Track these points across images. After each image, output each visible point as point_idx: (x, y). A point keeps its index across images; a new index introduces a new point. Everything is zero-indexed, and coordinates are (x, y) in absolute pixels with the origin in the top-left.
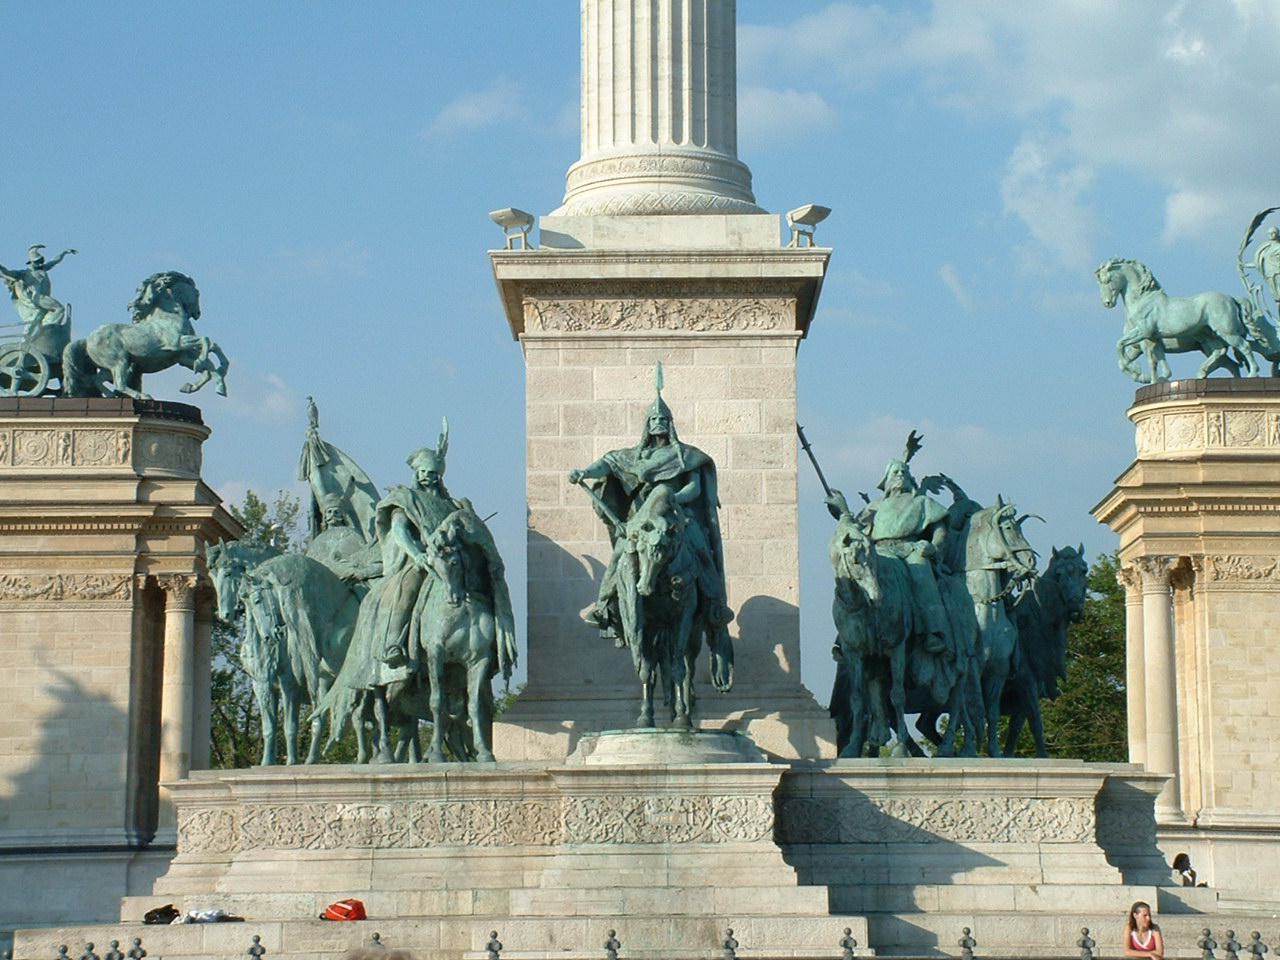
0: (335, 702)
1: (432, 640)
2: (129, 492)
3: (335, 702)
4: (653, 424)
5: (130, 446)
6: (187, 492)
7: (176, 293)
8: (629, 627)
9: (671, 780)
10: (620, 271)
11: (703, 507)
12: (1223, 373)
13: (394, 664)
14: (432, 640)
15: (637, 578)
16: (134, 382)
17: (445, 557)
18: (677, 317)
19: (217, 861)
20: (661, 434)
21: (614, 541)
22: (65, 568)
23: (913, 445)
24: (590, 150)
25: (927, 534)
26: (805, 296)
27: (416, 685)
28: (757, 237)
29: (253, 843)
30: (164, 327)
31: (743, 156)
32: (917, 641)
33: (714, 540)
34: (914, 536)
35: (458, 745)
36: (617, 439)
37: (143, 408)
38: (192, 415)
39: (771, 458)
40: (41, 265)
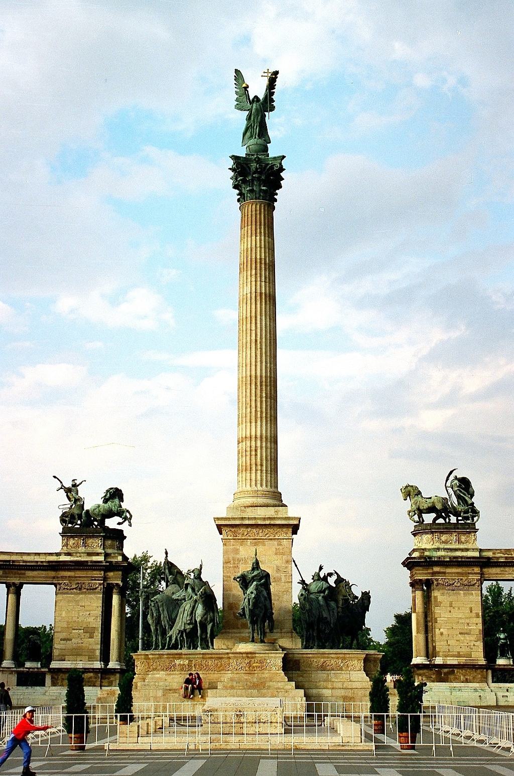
0: (173, 633)
1: (198, 620)
3: (173, 633)
4: (254, 564)
5: (102, 542)
6: (120, 558)
7: (116, 494)
8: (247, 617)
9: (257, 655)
10: (247, 522)
13: (189, 624)
14: (198, 620)
15: (249, 605)
16: (104, 522)
17: (202, 598)
18: (261, 534)
21: (244, 594)
23: (321, 568)
25: (324, 592)
27: (194, 629)
29: (154, 669)
30: (112, 505)
31: (279, 490)
33: (269, 593)
34: (320, 592)
36: (245, 568)
38: (121, 532)
39: (285, 570)
40: (75, 486)
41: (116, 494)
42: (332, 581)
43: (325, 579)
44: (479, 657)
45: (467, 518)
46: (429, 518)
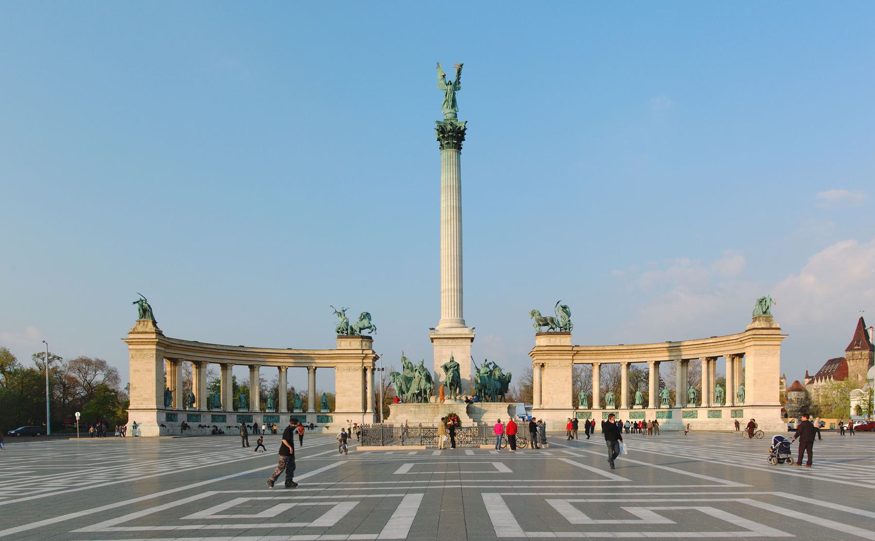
0: (409, 395)
2: (360, 352)
6: (371, 352)
11: (458, 370)
12: (551, 330)
19: (396, 415)
20: (452, 361)
22: (350, 365)
24: (443, 317)
26: (472, 339)
27: (421, 392)
28: (466, 331)
30: (365, 322)
32: (485, 387)
35: (426, 400)
36: (446, 361)
37: (363, 337)
38: (370, 338)
41: (367, 316)
42: (491, 367)
43: (487, 366)
44: (570, 405)
45: (566, 329)
46: (545, 329)
